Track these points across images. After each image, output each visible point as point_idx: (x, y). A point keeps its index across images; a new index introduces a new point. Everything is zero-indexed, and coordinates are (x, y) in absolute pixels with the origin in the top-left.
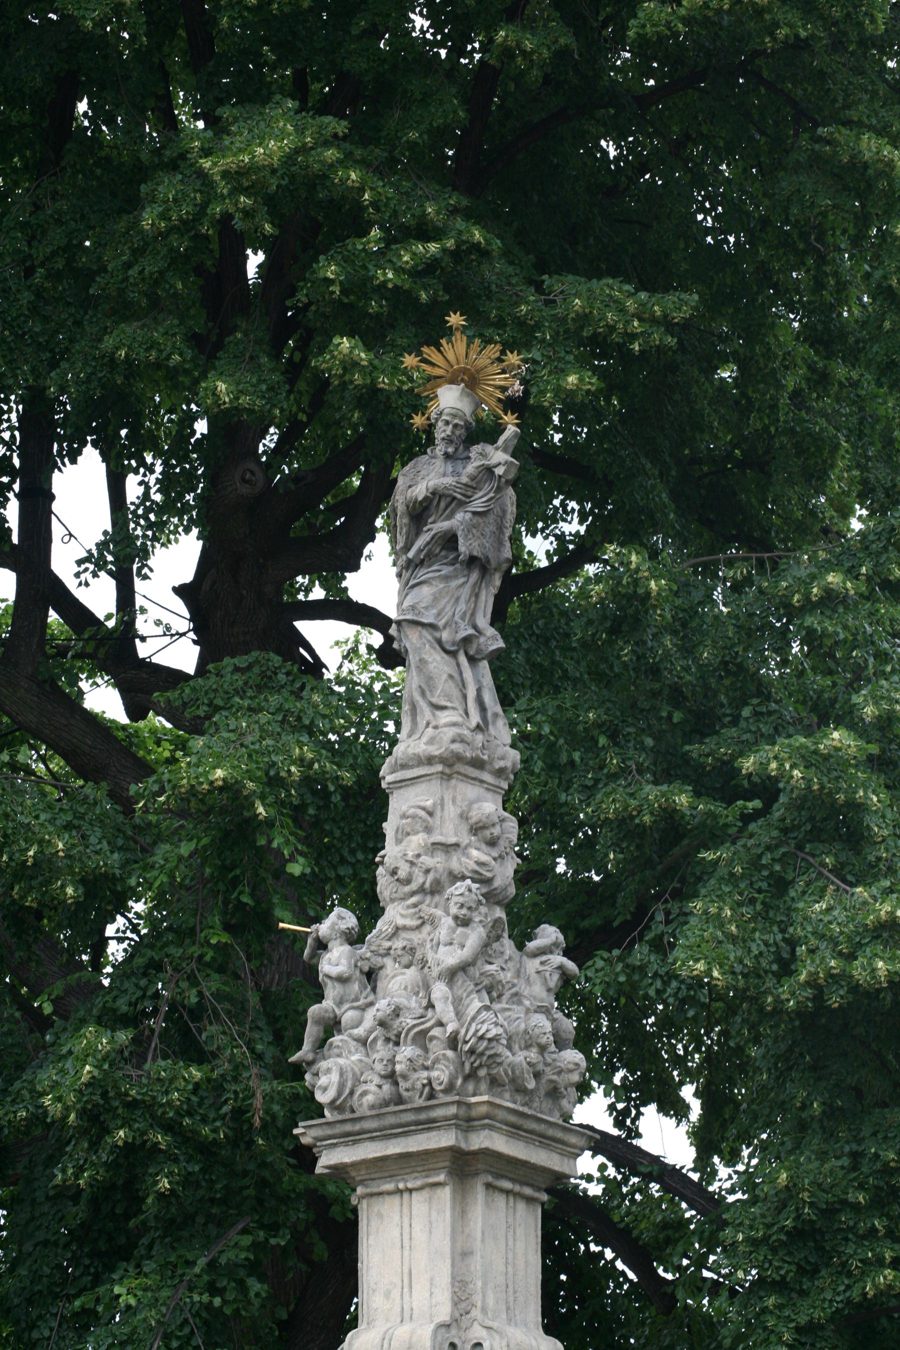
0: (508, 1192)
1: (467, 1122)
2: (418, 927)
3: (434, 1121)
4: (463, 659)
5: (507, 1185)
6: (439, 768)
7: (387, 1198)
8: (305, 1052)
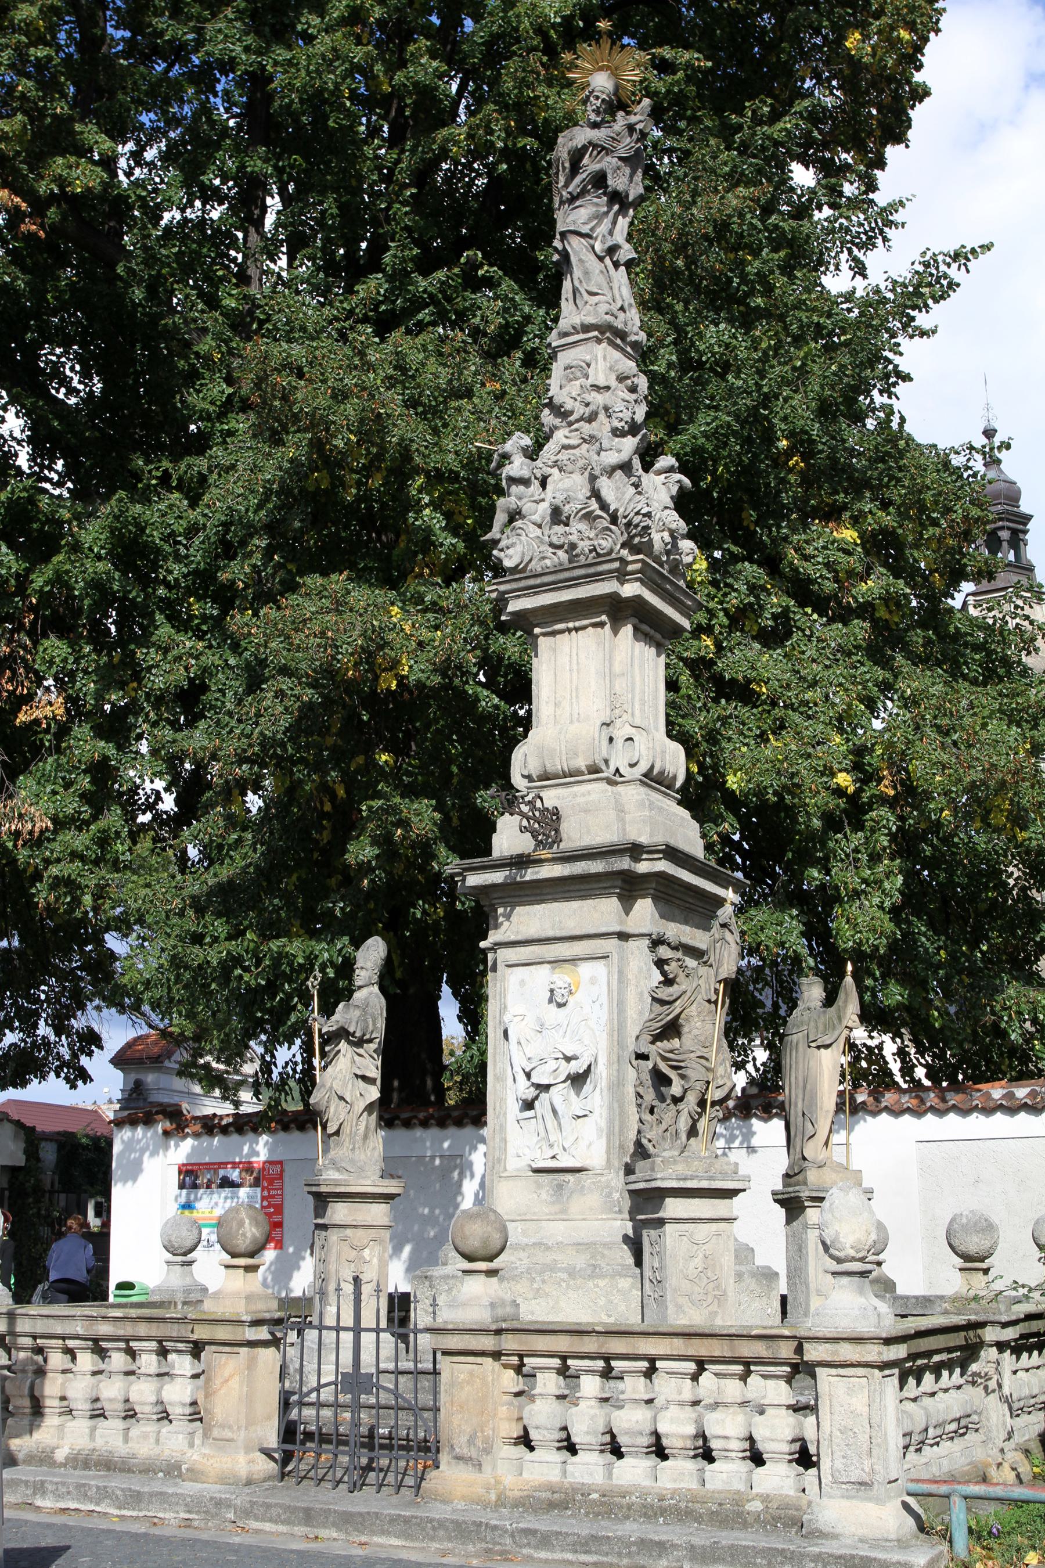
8: (494, 533)
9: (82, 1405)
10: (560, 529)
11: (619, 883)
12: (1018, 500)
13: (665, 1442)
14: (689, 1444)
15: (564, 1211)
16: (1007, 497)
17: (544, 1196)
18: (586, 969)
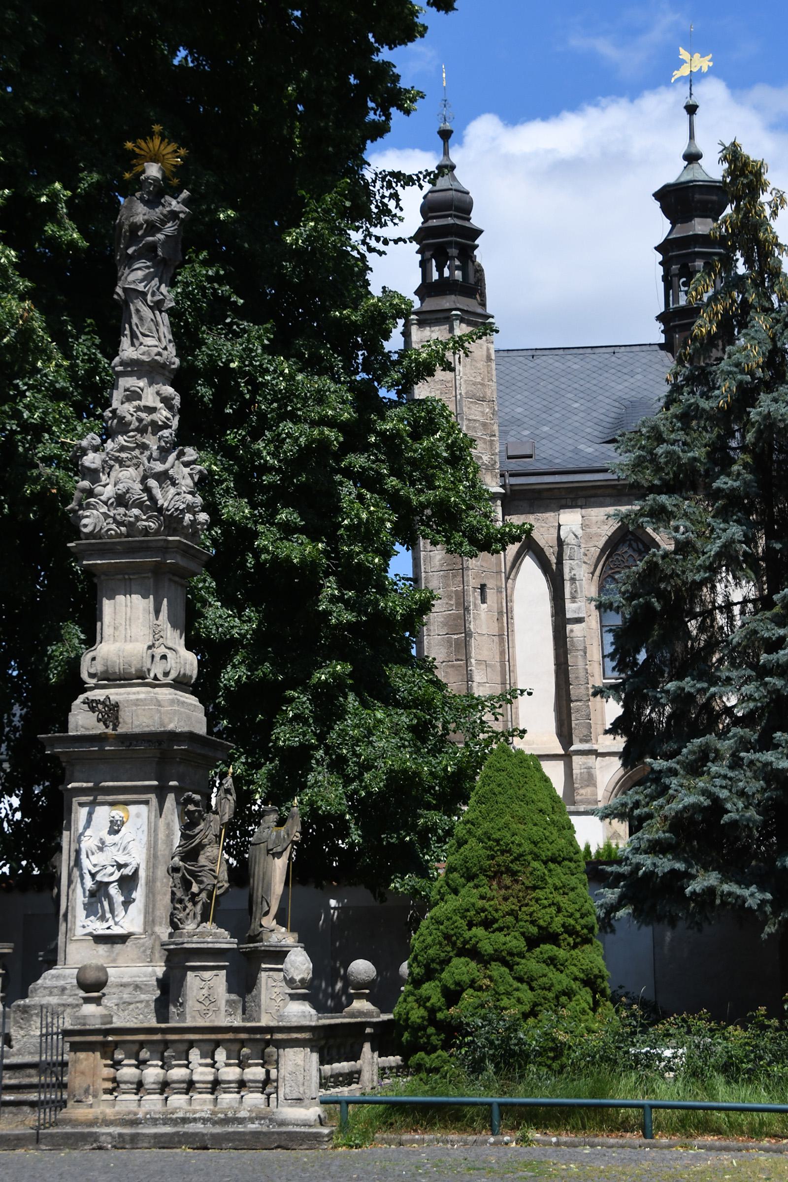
10: (122, 510)
12: (469, 211)
15: (114, 961)
16: (458, 209)
18: (132, 808)
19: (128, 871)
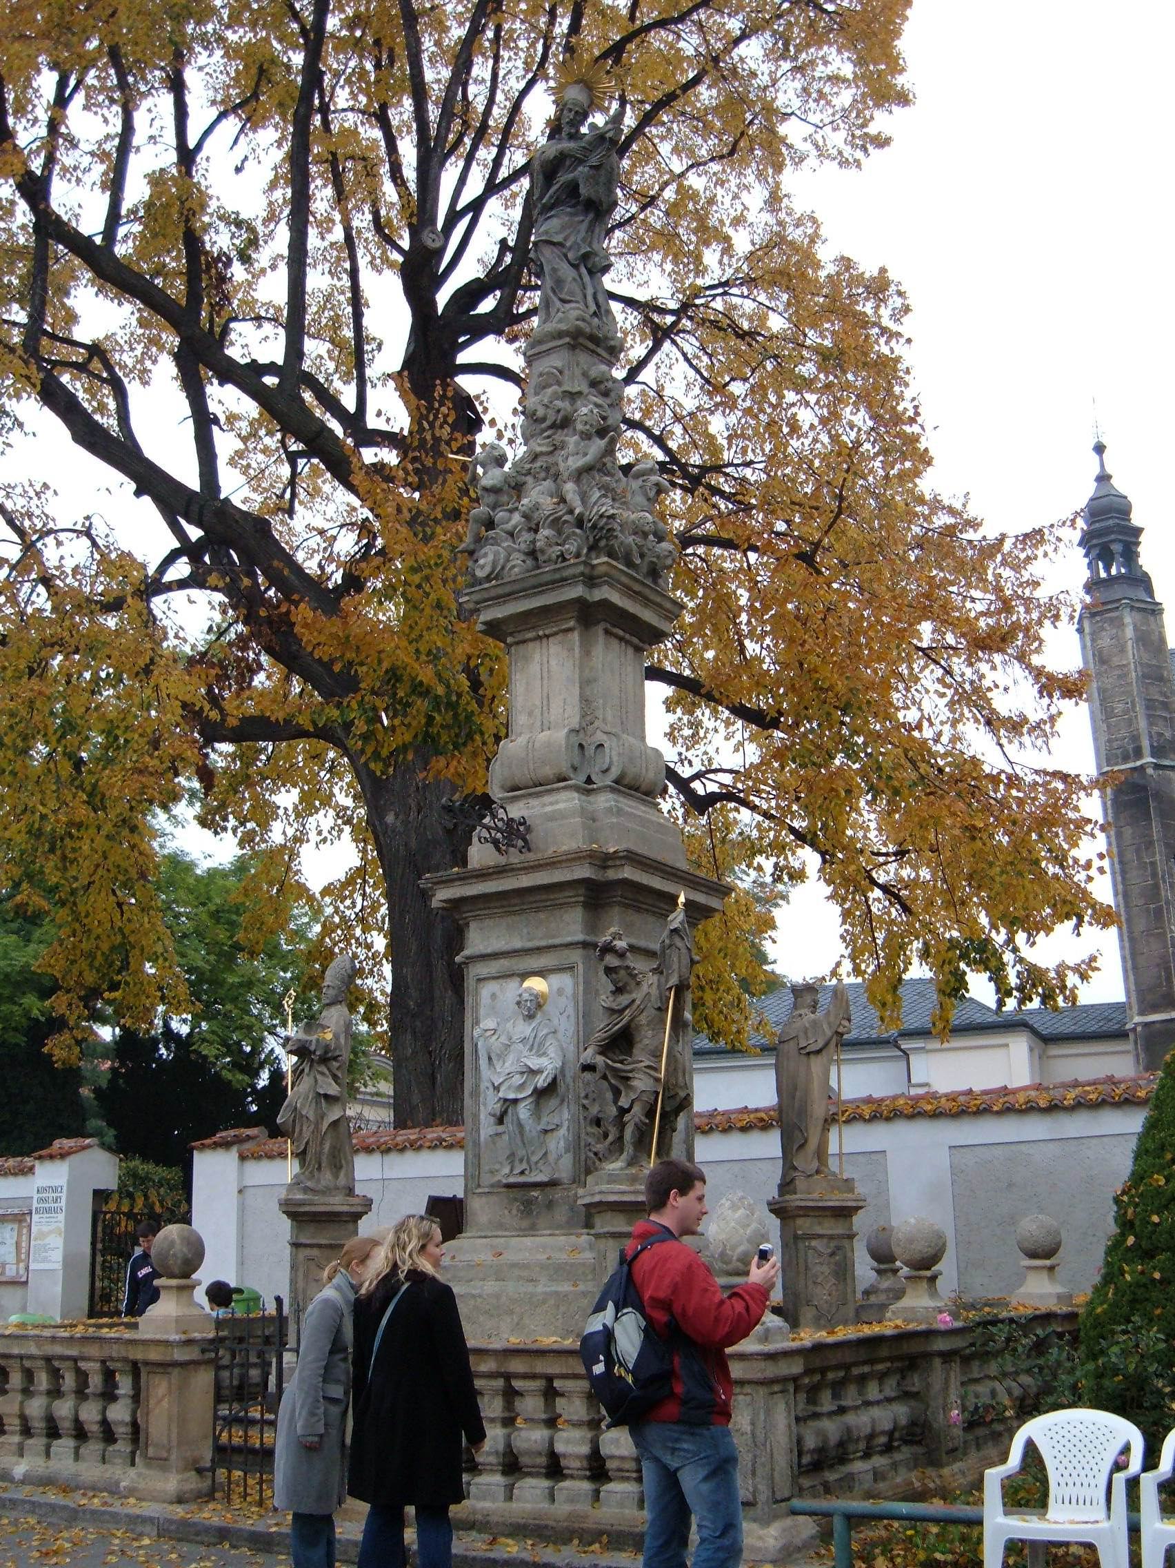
0: (621, 639)
1: (591, 581)
2: (551, 452)
3: (565, 579)
4: (583, 270)
5: (621, 633)
6: (567, 340)
7: (531, 645)
9: (38, 1425)
11: (582, 891)
13: (563, 1463)
14: (585, 1464)
16: (1119, 511)
17: (514, 1212)
19: (542, 1081)
